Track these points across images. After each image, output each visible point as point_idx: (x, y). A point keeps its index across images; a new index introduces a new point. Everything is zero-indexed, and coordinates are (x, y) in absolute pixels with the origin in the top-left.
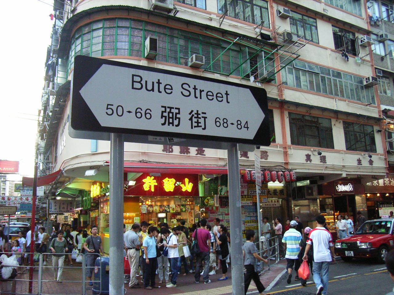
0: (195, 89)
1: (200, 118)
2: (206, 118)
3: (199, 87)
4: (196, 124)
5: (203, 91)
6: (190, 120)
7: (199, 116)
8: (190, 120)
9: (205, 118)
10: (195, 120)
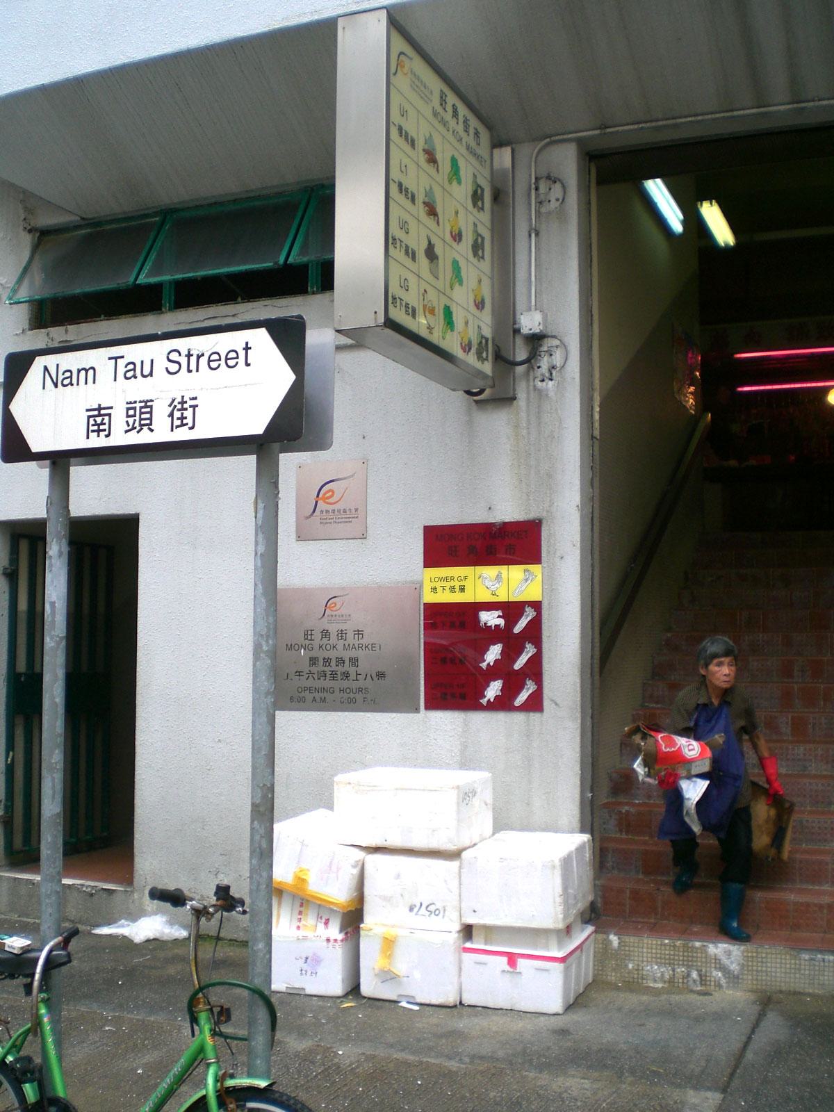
1: (186, 409)
2: (197, 406)
6: (169, 416)
7: (185, 406)
8: (169, 416)
9: (194, 407)
10: (177, 414)
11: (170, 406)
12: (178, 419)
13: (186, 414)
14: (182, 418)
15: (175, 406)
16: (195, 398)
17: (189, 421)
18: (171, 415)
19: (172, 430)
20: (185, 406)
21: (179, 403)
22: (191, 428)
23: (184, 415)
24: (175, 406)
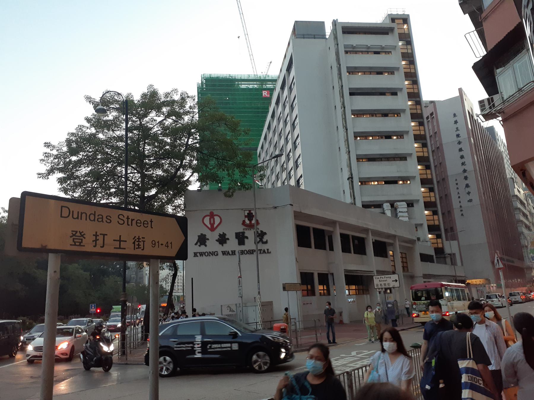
0: (128, 218)
3: (131, 218)
4: (137, 247)
7: (140, 240)
9: (144, 241)
10: (137, 243)
14: (139, 245)
17: (142, 246)
18: (134, 243)
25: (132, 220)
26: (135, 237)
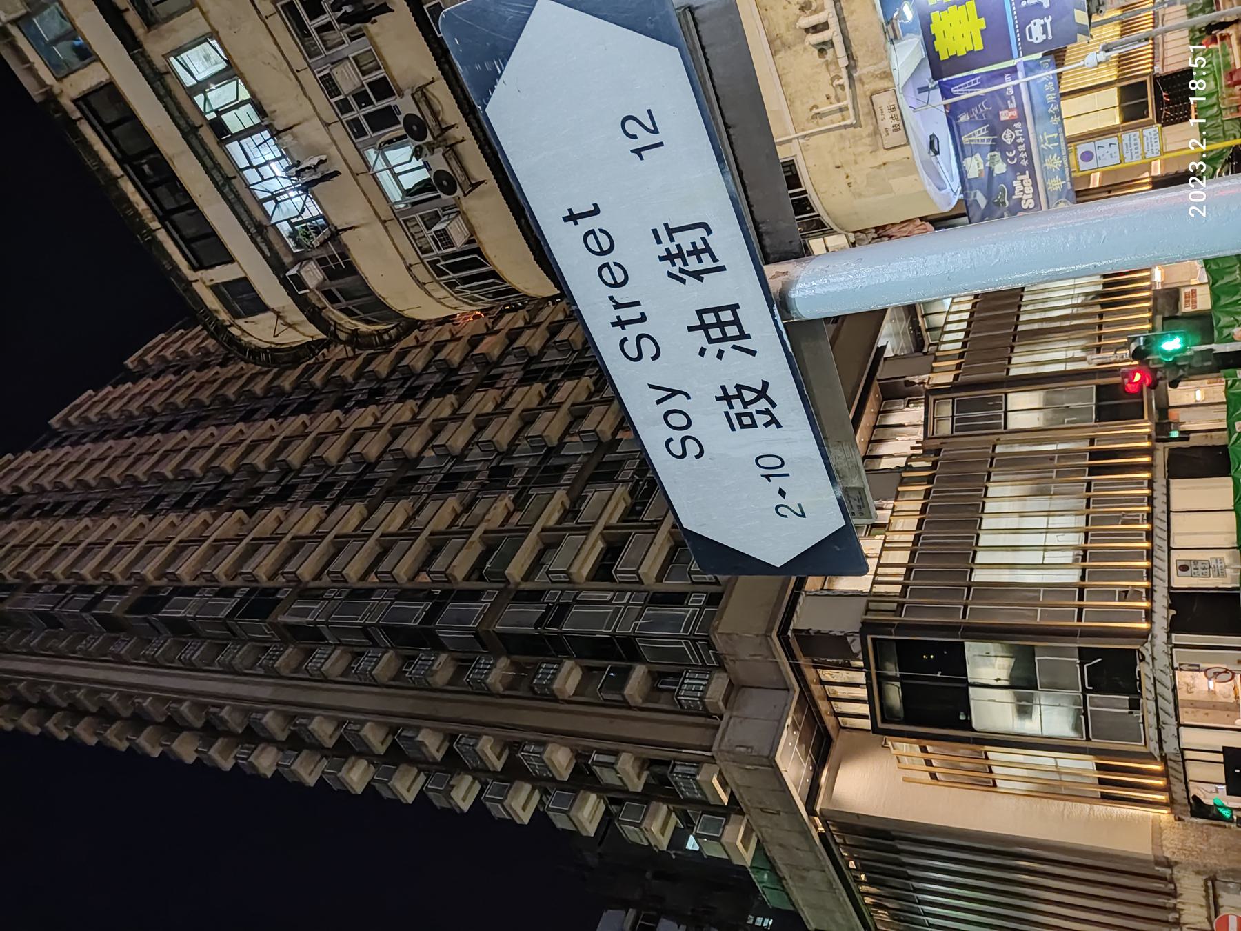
1: (679, 246)
2: (666, 225)
3: (613, 314)
5: (611, 298)
6: (701, 280)
7: (674, 251)
8: (701, 280)
9: (671, 232)
10: (693, 264)
11: (683, 281)
12: (700, 261)
13: (687, 247)
14: (696, 252)
15: (681, 270)
16: (655, 232)
18: (698, 275)
19: (723, 268)
20: (674, 251)
21: (673, 264)
22: (709, 232)
23: (691, 249)
24: (681, 270)
25: (618, 306)
26: (670, 275)
